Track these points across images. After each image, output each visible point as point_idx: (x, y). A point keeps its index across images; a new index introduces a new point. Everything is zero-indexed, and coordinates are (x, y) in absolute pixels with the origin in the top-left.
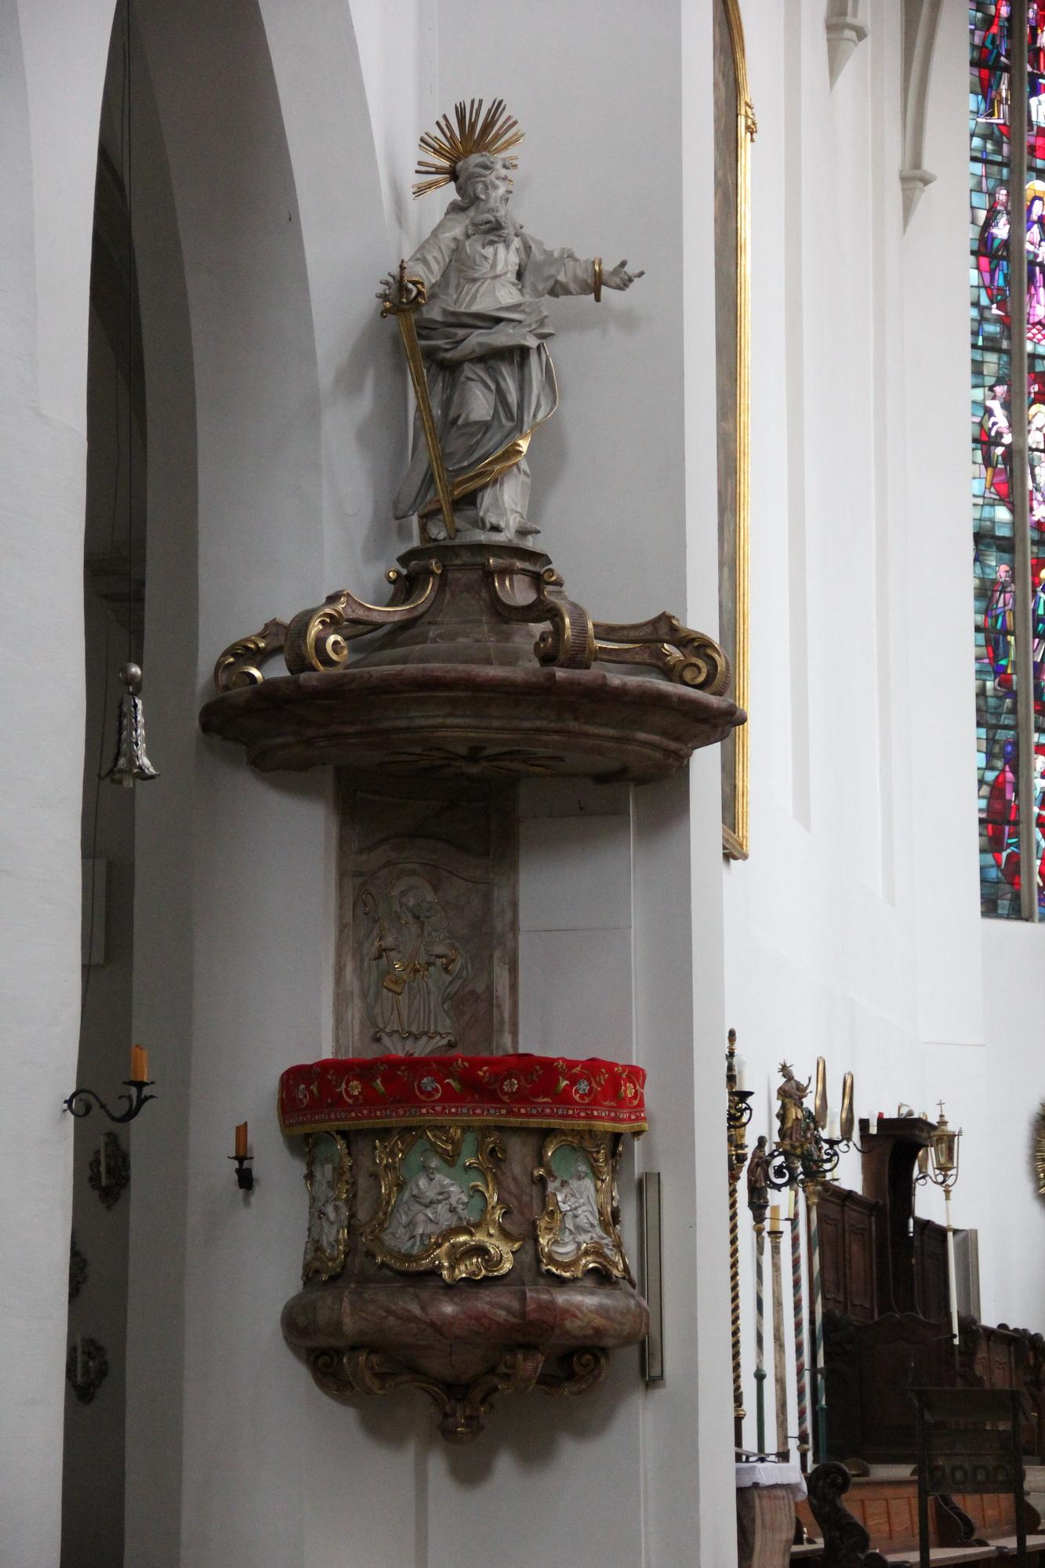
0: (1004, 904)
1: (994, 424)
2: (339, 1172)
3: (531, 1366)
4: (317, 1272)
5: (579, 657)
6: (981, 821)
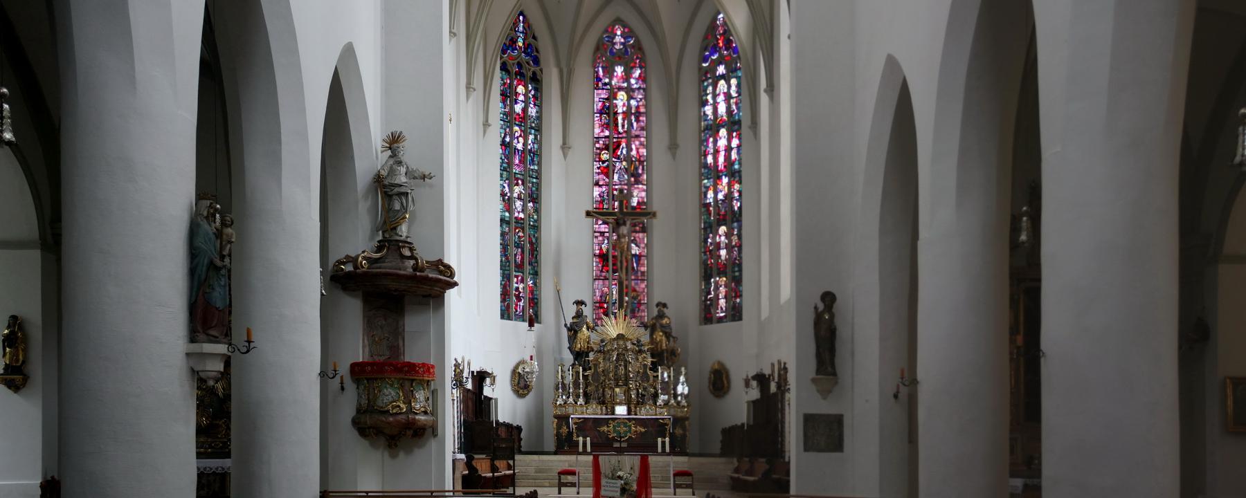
0: (506, 316)
2: (365, 387)
3: (410, 433)
4: (360, 410)
5: (422, 270)
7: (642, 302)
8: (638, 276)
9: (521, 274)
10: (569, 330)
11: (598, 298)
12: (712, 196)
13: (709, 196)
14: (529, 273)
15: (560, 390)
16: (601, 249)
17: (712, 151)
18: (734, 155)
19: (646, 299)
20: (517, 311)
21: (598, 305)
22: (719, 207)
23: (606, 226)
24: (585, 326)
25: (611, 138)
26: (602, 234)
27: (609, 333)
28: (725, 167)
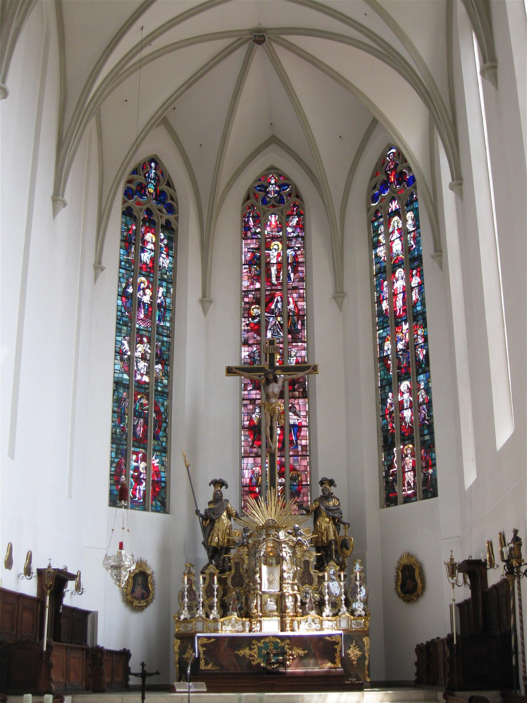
1: (125, 348)
6: (111, 475)
7: (304, 483)
8: (298, 451)
9: (143, 451)
10: (204, 518)
11: (248, 480)
12: (390, 347)
13: (386, 348)
14: (154, 450)
15: (186, 600)
16: (251, 420)
17: (387, 296)
18: (415, 296)
19: (308, 479)
20: (135, 496)
21: (247, 489)
22: (399, 359)
23: (258, 391)
24: (225, 514)
25: (263, 290)
26: (253, 401)
27: (256, 520)
28: (404, 311)
